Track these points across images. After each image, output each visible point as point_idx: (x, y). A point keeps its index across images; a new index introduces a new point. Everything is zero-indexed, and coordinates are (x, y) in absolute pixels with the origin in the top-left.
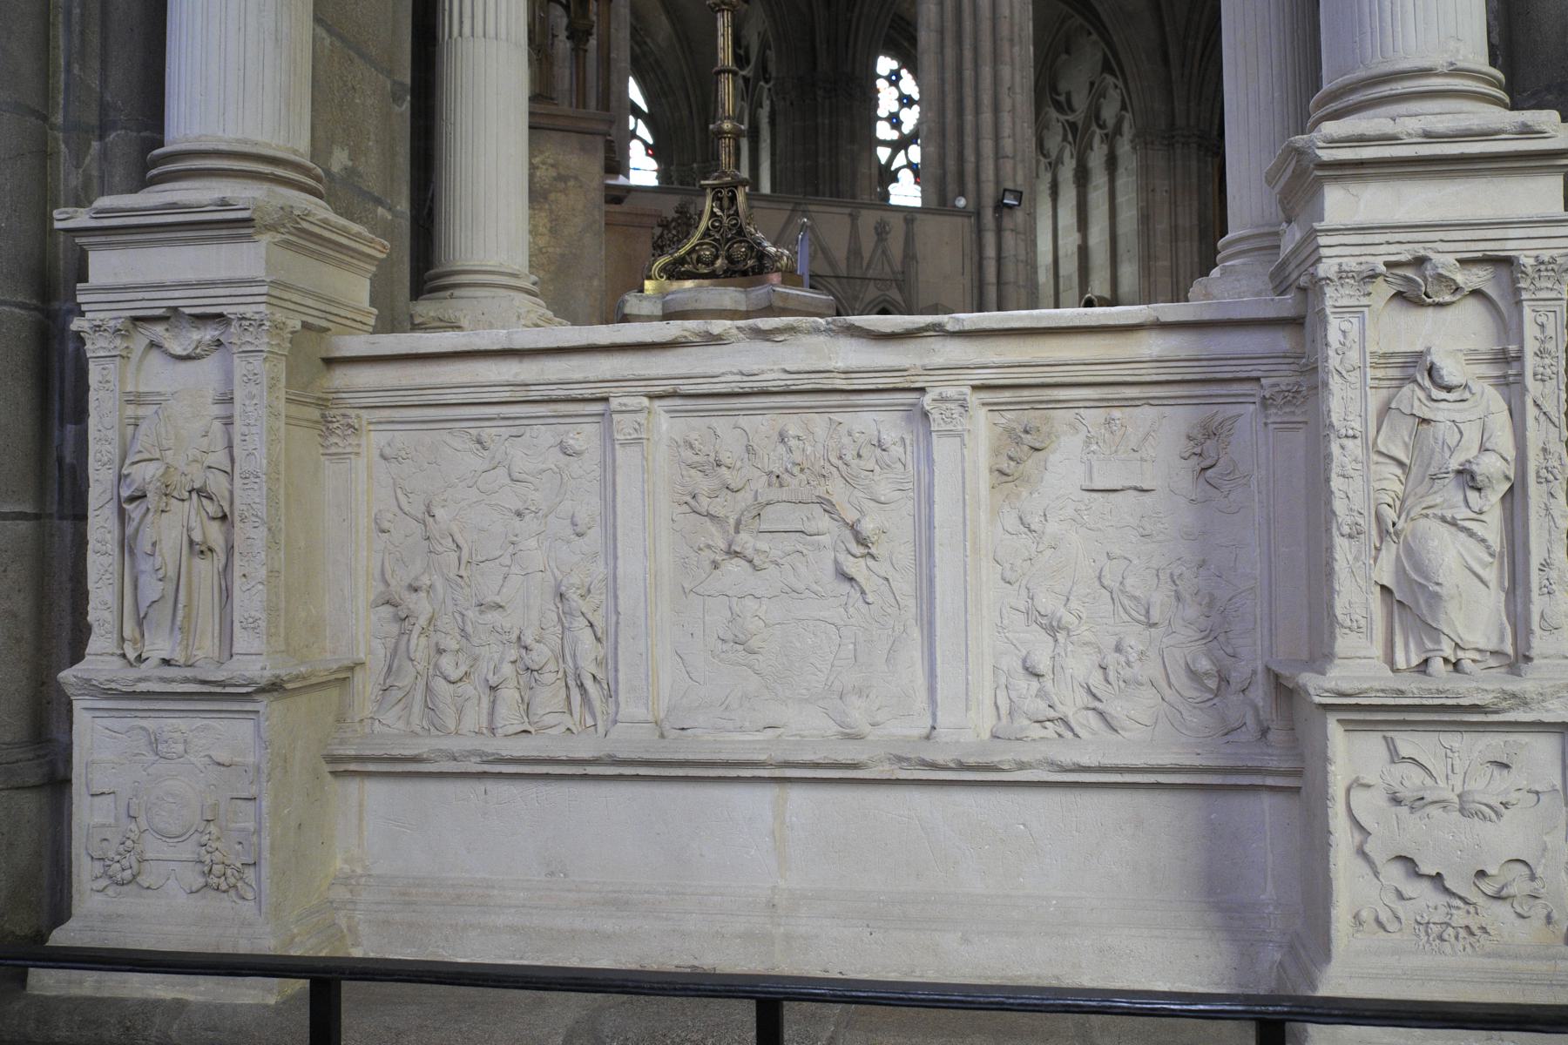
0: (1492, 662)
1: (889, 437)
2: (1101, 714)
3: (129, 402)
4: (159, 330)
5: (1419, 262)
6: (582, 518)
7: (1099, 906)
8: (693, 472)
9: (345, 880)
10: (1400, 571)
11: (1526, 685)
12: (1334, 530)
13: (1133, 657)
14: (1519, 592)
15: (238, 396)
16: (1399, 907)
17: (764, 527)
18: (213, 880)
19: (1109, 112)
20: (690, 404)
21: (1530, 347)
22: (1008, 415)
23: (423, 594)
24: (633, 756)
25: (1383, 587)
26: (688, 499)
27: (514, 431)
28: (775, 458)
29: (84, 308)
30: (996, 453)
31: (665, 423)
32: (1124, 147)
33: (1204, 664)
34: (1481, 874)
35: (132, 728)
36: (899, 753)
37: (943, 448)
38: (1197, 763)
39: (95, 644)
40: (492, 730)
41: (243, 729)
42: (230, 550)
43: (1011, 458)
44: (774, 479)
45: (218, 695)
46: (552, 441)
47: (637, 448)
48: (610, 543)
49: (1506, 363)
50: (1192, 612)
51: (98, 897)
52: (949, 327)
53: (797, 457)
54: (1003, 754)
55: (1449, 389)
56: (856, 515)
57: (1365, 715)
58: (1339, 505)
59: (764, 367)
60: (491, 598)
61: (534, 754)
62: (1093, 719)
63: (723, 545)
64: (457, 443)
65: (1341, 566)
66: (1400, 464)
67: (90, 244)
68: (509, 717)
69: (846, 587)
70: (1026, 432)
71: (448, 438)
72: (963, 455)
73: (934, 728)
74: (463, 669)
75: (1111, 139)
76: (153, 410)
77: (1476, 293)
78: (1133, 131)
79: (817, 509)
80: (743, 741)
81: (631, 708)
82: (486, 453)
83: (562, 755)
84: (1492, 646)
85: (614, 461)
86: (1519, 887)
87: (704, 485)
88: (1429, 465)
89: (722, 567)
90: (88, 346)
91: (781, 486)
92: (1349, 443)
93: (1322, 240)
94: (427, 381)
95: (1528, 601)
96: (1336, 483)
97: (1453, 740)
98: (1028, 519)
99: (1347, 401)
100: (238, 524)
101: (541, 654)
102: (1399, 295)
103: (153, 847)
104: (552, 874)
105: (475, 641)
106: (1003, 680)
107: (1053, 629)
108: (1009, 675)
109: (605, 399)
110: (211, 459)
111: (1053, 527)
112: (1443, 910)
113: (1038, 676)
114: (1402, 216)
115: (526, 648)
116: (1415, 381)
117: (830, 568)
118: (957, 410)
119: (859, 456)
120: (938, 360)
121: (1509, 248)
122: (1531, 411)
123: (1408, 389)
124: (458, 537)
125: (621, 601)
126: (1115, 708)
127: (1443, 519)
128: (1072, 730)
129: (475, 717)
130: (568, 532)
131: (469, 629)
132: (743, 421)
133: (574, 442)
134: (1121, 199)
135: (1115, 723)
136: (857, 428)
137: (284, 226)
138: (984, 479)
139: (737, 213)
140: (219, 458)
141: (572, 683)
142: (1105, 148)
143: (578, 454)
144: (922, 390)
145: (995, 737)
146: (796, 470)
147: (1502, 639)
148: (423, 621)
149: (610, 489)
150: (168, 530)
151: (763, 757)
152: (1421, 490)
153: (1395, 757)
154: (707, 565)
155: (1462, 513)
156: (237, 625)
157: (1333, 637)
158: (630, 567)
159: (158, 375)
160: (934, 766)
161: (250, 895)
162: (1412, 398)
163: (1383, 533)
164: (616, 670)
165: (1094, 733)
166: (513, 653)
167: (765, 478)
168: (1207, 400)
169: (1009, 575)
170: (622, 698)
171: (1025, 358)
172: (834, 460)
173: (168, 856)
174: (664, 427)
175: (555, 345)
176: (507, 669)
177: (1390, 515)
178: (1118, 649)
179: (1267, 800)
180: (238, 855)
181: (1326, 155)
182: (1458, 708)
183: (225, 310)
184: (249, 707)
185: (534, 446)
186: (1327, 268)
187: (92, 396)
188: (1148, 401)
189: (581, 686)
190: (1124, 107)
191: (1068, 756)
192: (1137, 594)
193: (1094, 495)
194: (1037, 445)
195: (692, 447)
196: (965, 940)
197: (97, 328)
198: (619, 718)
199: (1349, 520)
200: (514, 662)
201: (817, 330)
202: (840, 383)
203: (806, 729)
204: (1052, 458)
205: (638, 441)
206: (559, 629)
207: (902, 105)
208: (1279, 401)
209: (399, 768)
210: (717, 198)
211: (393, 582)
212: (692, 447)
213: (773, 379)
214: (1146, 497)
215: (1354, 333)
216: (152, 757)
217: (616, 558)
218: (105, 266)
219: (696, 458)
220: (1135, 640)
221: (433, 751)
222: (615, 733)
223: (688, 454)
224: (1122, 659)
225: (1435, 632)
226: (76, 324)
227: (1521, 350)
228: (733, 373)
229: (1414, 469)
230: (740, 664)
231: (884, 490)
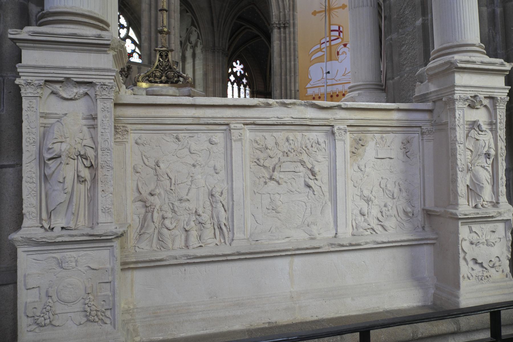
0: (490, 205)
1: (321, 141)
2: (382, 226)
3: (41, 117)
4: (58, 86)
5: (475, 97)
6: (218, 167)
7: (380, 285)
8: (257, 151)
9: (127, 311)
10: (471, 180)
11: (501, 210)
12: (458, 170)
13: (390, 208)
14: (495, 185)
15: (100, 117)
16: (472, 272)
17: (282, 170)
18: (91, 318)
19: (193, 39)
20: (258, 127)
21: (499, 121)
22: (355, 135)
23: (156, 197)
24: (247, 251)
25: (468, 186)
26: (256, 160)
27: (191, 135)
28: (285, 147)
29: (20, 74)
30: (351, 146)
31: (248, 134)
32: (198, 50)
33: (409, 209)
34: (491, 261)
35: (49, 258)
36: (331, 242)
37: (339, 144)
38: (413, 238)
40: (187, 247)
41: (105, 254)
42: (94, 179)
43: (356, 148)
44: (285, 154)
45: (97, 240)
46: (206, 139)
47: (240, 142)
48: (230, 177)
49: (492, 124)
50: (404, 194)
51: (30, 334)
52: (343, 106)
53: (292, 146)
54: (361, 240)
55: (482, 131)
56: (311, 166)
57: (469, 220)
58: (459, 162)
59: (285, 116)
60: (185, 197)
61: (209, 254)
62: (380, 228)
63: (268, 177)
64: (167, 138)
65: (459, 180)
66: (471, 151)
67: (24, 47)
68: (194, 241)
69: (308, 190)
70: (360, 140)
71: (164, 137)
72: (345, 148)
73: (336, 234)
74: (174, 224)
75: (194, 47)
76: (51, 120)
77: (485, 106)
78: (202, 46)
79: (299, 164)
80: (280, 243)
81: (238, 235)
82: (180, 143)
83: (220, 253)
84: (490, 200)
85: (231, 146)
86: (497, 264)
87: (262, 156)
88: (478, 152)
89: (268, 184)
90: (23, 91)
91: (288, 156)
92: (461, 145)
93: (456, 89)
94: (157, 115)
95: (499, 188)
96: (458, 156)
97: (483, 226)
98: (361, 167)
99: (460, 133)
100: (100, 169)
101: (205, 217)
102: (469, 105)
103: (59, 308)
104: (211, 298)
105: (178, 213)
106: (354, 217)
107: (368, 201)
108: (356, 216)
109: (228, 124)
110: (85, 142)
111: (367, 169)
112: (481, 272)
113: (364, 215)
114: (472, 83)
115: (199, 215)
116: (474, 129)
117: (303, 183)
118: (343, 133)
119: (312, 146)
120: (338, 117)
121: (495, 95)
122: (499, 138)
123: (473, 131)
124: (170, 175)
125: (234, 197)
126: (386, 224)
127: (482, 166)
128: (375, 231)
129: (180, 242)
130: (213, 172)
131: (176, 209)
132: (275, 134)
133: (215, 139)
134: (197, 67)
135: (386, 229)
136: (311, 137)
137: (117, 49)
138: (348, 154)
139: (168, 61)
140: (88, 142)
141: (216, 227)
142: (192, 50)
143: (216, 144)
144: (332, 126)
145: (353, 235)
146: (292, 151)
147: (492, 198)
148: (157, 207)
149: (229, 157)
150: (68, 171)
151: (291, 248)
152: (476, 159)
153: (471, 231)
154: (262, 183)
155: (486, 165)
156: (100, 211)
157: (458, 200)
158: (237, 184)
159: (55, 106)
160: (343, 246)
161: (108, 321)
162: (473, 133)
163: (469, 170)
164: (233, 221)
165: (381, 232)
166: (194, 218)
167: (281, 153)
168: (404, 132)
169: (356, 185)
170: (235, 232)
171: (362, 117)
172: (304, 148)
173: (68, 311)
174: (248, 135)
175: (212, 104)
176: (192, 224)
177: (470, 165)
178: (385, 206)
179: (425, 248)
180: (103, 305)
181: (460, 65)
182: (489, 217)
184: (109, 244)
185: (199, 141)
186: (456, 96)
188: (392, 132)
189: (220, 228)
190: (198, 38)
191: (379, 239)
192: (390, 189)
193: (378, 160)
194: (363, 144)
195: (257, 142)
196: (353, 299)
197: (29, 84)
198: (235, 238)
199: (461, 167)
200: (194, 221)
201: (301, 105)
202: (309, 123)
203: (298, 237)
204: (367, 148)
205: (240, 140)
206: (210, 208)
207: (121, 28)
208: (427, 133)
209: (152, 264)
210: (161, 56)
211: (143, 193)
212: (257, 142)
213: (288, 120)
214: (391, 160)
215: (461, 115)
216: (59, 269)
217: (232, 181)
218: (30, 57)
219: (258, 146)
220: (390, 204)
221: (168, 257)
222: (234, 244)
223: (255, 145)
224: (387, 209)
225: (479, 196)
227: (496, 122)
228: (274, 117)
229: (474, 153)
230: (274, 217)
231: (320, 158)
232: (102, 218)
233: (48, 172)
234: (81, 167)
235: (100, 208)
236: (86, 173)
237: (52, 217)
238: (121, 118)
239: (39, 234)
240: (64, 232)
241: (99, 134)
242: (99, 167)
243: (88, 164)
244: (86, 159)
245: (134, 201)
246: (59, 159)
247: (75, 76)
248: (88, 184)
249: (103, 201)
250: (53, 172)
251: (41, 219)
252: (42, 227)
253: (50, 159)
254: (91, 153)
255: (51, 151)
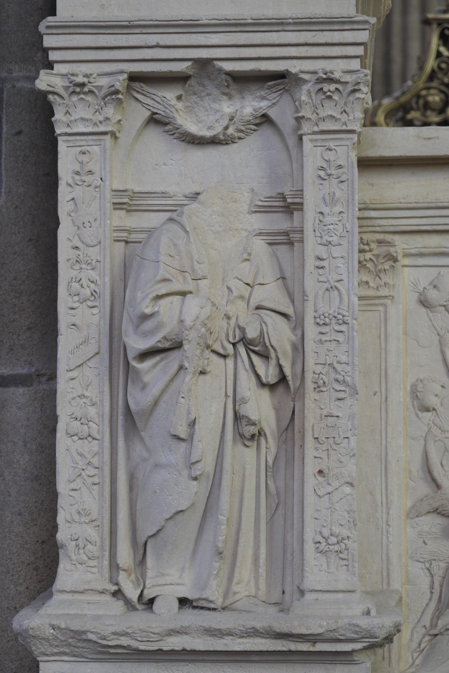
3: (118, 206)
4: (169, 94)
15: (311, 200)
39: (68, 575)
42: (290, 427)
100: (311, 395)
110: (260, 296)
140: (271, 294)
150: (206, 396)
156: (309, 547)
159: (161, 167)
183: (293, 67)
187: (64, 193)
197: (78, 88)
226: (44, 81)
232: (317, 572)
233: (139, 400)
234: (247, 383)
235: (310, 534)
236: (261, 407)
237: (150, 561)
238: (373, 214)
239: (107, 618)
240: (190, 618)
241: (310, 263)
242: (309, 385)
243: (269, 374)
244: (265, 357)
245: (414, 513)
246: (175, 355)
247: (232, 53)
248: (270, 446)
249: (322, 509)
250: (156, 403)
251: (114, 567)
252: (118, 594)
253: (144, 355)
254: (280, 334)
255: (149, 325)
